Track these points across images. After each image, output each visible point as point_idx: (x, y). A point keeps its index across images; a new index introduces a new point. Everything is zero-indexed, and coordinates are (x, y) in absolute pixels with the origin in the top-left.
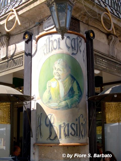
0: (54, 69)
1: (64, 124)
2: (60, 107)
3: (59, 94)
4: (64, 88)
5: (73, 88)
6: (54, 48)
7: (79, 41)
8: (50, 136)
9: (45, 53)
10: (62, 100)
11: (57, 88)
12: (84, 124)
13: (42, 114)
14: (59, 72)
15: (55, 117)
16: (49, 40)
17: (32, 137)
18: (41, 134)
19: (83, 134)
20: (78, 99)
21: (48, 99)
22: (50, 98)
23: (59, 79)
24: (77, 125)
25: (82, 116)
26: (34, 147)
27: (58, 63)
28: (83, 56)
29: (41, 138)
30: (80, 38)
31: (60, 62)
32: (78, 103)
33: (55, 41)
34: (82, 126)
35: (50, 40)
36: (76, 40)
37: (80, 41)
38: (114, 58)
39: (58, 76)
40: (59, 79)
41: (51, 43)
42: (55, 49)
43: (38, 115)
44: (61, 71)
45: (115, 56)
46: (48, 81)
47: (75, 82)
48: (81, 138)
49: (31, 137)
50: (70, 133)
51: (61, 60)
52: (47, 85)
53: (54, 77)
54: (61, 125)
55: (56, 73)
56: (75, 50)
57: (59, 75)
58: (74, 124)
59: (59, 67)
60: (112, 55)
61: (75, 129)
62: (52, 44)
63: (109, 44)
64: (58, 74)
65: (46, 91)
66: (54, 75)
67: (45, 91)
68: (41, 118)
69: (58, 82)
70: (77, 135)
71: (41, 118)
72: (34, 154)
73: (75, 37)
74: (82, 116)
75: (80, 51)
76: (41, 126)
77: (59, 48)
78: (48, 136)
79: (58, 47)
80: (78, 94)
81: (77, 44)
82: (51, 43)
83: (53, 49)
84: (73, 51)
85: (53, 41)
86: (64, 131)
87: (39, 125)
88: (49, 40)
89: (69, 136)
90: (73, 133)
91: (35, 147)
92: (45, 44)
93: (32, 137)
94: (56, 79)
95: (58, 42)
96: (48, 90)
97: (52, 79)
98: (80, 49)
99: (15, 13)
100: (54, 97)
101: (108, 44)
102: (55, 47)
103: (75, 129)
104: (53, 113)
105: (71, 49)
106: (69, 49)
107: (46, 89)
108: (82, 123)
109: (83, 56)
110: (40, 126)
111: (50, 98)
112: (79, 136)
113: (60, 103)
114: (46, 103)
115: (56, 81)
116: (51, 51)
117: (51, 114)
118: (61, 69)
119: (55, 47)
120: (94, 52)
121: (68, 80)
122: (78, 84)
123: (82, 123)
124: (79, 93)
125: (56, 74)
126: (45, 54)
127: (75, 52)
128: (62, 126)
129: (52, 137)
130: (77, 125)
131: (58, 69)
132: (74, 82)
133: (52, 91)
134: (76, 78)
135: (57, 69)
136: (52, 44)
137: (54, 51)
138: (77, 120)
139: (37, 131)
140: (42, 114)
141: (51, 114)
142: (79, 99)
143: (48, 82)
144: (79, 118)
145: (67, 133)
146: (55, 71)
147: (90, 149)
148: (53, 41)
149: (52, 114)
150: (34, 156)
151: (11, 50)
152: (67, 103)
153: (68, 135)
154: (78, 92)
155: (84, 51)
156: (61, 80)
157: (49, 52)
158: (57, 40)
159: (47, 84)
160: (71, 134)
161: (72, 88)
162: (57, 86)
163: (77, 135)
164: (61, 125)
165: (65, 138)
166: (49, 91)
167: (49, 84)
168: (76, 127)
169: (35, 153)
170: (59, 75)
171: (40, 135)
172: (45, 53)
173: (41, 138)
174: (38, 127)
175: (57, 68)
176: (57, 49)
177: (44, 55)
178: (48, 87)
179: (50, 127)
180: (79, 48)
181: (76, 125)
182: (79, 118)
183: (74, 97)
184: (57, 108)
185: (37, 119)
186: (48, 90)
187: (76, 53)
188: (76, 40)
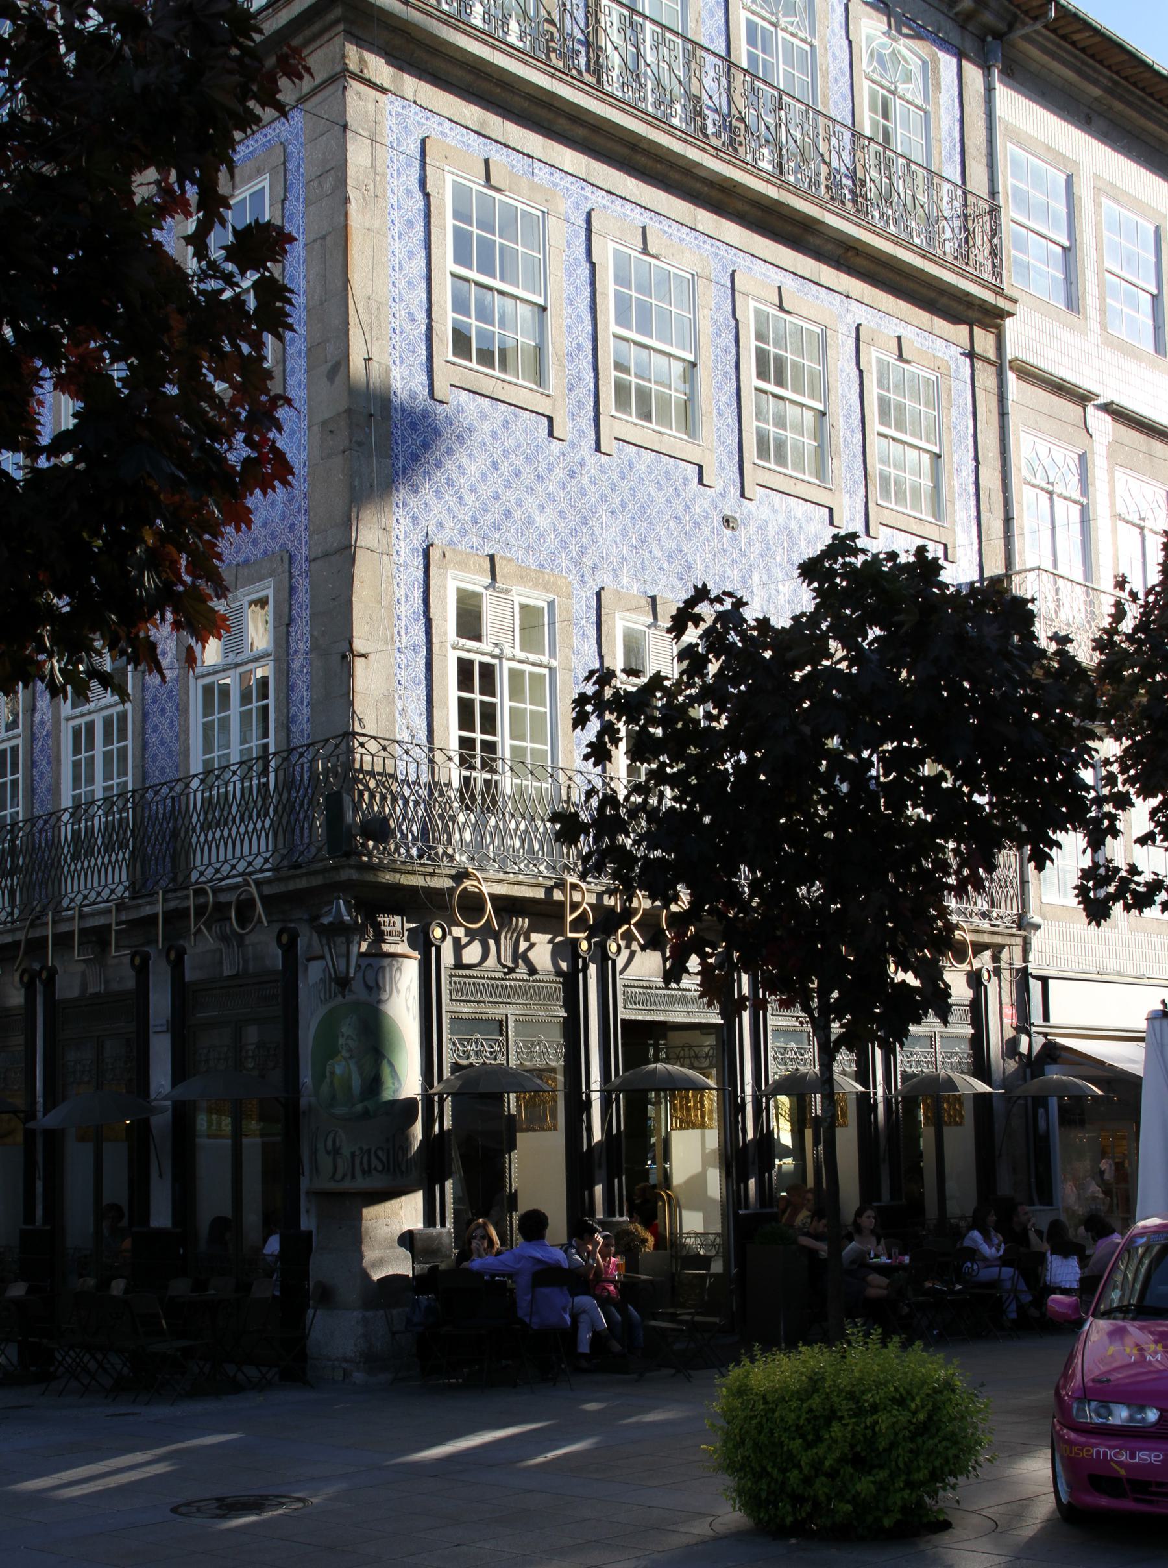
1: (361, 1149)
3: (350, 1088)
14: (350, 1042)
23: (351, 1057)
40: (351, 1057)
52: (328, 1069)
61: (384, 1159)
72: (307, 1212)
86: (361, 1163)
90: (380, 1168)
94: (345, 1058)
96: (328, 1080)
99: (253, 889)
103: (384, 1159)
115: (344, 1063)
129: (339, 1176)
131: (348, 1037)
145: (366, 1167)
146: (341, 1041)
153: (370, 1171)
160: (375, 1168)
166: (332, 1082)
170: (350, 1050)
178: (328, 1074)
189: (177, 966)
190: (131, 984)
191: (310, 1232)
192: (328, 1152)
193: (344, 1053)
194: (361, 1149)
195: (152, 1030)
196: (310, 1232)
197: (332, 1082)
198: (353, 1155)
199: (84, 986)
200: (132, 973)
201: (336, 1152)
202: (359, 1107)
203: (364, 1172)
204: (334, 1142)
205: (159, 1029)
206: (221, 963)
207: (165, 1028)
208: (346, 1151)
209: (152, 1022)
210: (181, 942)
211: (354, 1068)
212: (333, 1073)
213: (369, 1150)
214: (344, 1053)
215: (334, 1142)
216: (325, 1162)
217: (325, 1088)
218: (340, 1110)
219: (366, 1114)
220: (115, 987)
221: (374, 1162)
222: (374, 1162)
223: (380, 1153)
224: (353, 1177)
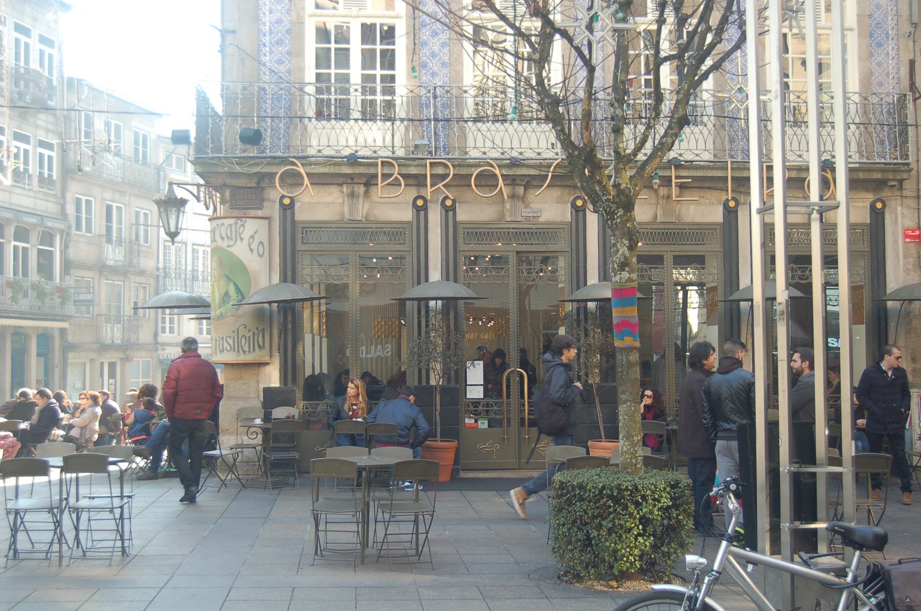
34: (243, 340)
36: (234, 226)
47: (232, 284)
61: (231, 343)
73: (232, 221)
90: (229, 348)
112: (238, 351)
127: (231, 243)
188: (234, 226)
221: (226, 345)
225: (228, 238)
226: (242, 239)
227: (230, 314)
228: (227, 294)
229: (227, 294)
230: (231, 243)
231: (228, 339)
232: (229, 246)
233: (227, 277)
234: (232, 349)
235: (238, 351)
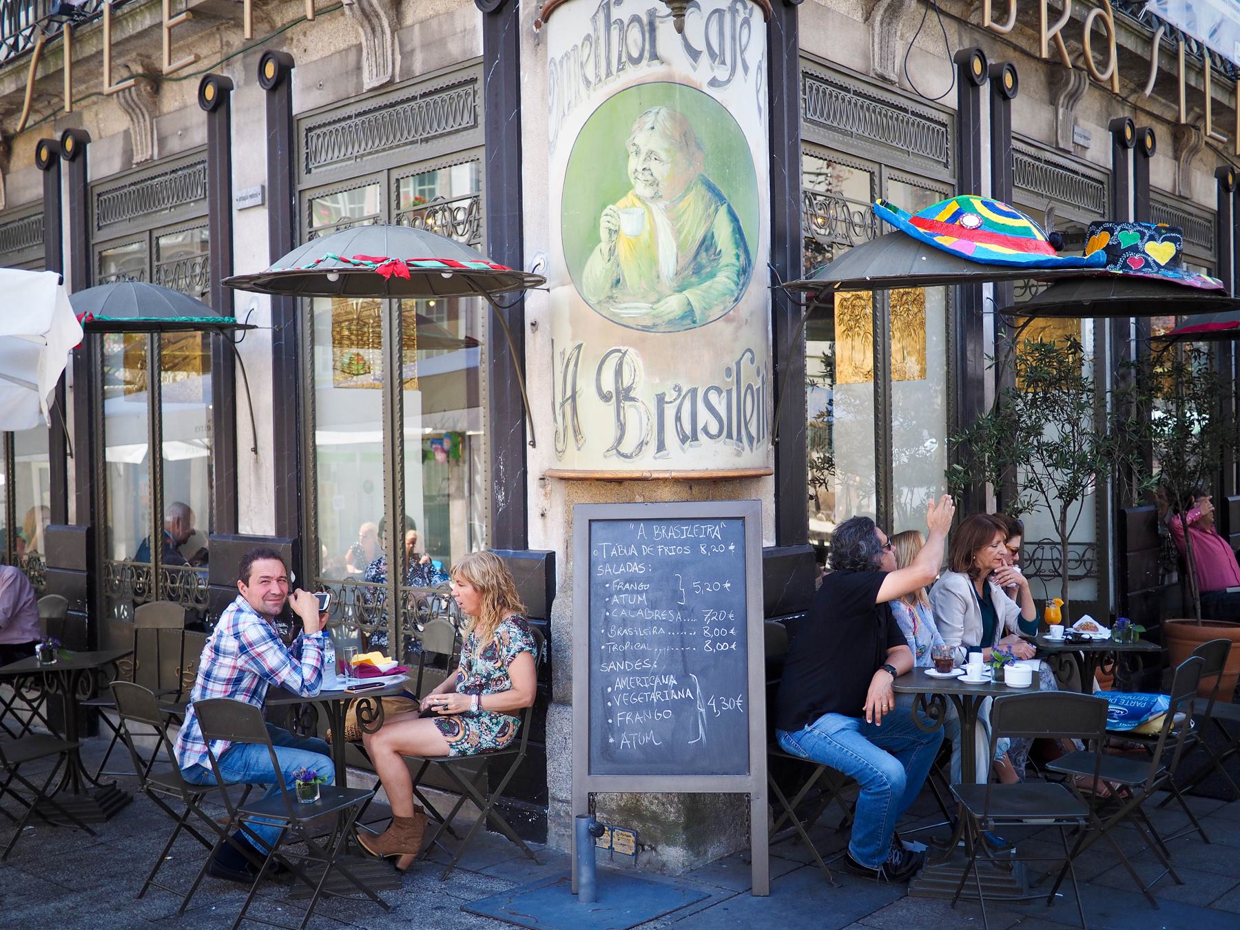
0: (632, 156)
1: (678, 389)
2: (658, 321)
3: (654, 262)
4: (677, 238)
5: (713, 237)
6: (630, 57)
7: (739, 20)
8: (619, 441)
9: (591, 78)
10: (668, 292)
11: (645, 236)
12: (758, 390)
13: (579, 347)
14: (653, 165)
15: (640, 363)
16: (608, 17)
17: (534, 445)
18: (577, 431)
19: (754, 432)
20: (733, 286)
21: (608, 286)
22: (618, 281)
23: (656, 197)
24: (729, 392)
25: (748, 355)
26: (544, 486)
27: (649, 125)
28: (758, 92)
29: (579, 449)
30: (745, 7)
31: (656, 119)
32: (736, 300)
33: (636, 24)
35: (613, 20)
36: (728, 17)
37: (746, 21)
38: (892, 83)
39: (651, 185)
41: (615, 33)
42: (636, 61)
43: (563, 353)
44: (661, 161)
45: (894, 77)
46: (604, 206)
47: (723, 210)
48: (743, 449)
49: (529, 448)
50: (700, 426)
51: (663, 111)
53: (630, 187)
54: (664, 394)
55: (640, 169)
56: (723, 63)
57: (654, 183)
58: (719, 391)
59: (652, 146)
60: (879, 71)
62: (623, 39)
63: (868, 17)
64: (649, 178)
65: (597, 249)
66: (632, 181)
67: (592, 250)
68: (576, 365)
69: (650, 212)
70: (730, 436)
71: (576, 365)
74: (748, 355)
75: (746, 68)
76: (578, 400)
77: (654, 56)
78: (611, 441)
79: (647, 54)
80: (734, 261)
81: (733, 38)
82: (615, 33)
83: (624, 59)
84: (712, 69)
85: (626, 22)
86: (678, 419)
87: (569, 393)
88: (608, 17)
89: (697, 439)
90: (714, 428)
91: (549, 488)
92: (589, 36)
93: (534, 445)
95: (647, 28)
96: (604, 246)
97: (624, 199)
98: (744, 61)
100: (631, 276)
101: (866, 20)
102: (635, 55)
104: (631, 346)
105: (705, 58)
106: (695, 61)
107: (600, 241)
108: (750, 387)
109: (758, 92)
110: (573, 397)
111: (618, 281)
112: (739, 439)
113: (658, 301)
114: (599, 302)
115: (640, 209)
116: (619, 70)
117: (619, 351)
118: (663, 155)
119: (635, 55)
120: (803, 66)
121: (694, 205)
122: (734, 219)
123: (750, 387)
124: (738, 257)
125: (640, 176)
126: (588, 83)
127: (722, 74)
128: (667, 399)
129: (628, 446)
130: (729, 392)
132: (717, 210)
133: (622, 250)
134: (724, 193)
135: (643, 156)
136: (623, 39)
137: (630, 68)
138: (729, 371)
139: (560, 419)
140: (579, 347)
141: (619, 351)
142: (737, 284)
143: (605, 212)
144: (738, 364)
145: (688, 429)
146: (634, 163)
147: (777, 495)
148: (626, 22)
149: (623, 349)
150: (545, 526)
151: (413, 51)
152: (689, 304)
153: (695, 437)
154: (735, 251)
155: (759, 68)
156: (662, 204)
157: (609, 74)
158: (645, 19)
159: (603, 219)
160: (705, 430)
161: (709, 235)
162: (648, 227)
163: (730, 436)
164: (664, 394)
165: (683, 449)
166: (612, 251)
167: (609, 218)
168: (724, 402)
169: (548, 514)
170: (654, 183)
171: (576, 436)
172: (590, 72)
173: (579, 449)
174: (562, 405)
175: (644, 150)
176: (644, 62)
177: (582, 86)
178: (604, 234)
179: (618, 402)
180: (742, 52)
181: (724, 394)
182: (738, 364)
183: (719, 274)
184: (649, 323)
185: (559, 368)
186: (604, 246)
187: (729, 81)
188: (728, 17)
189: (279, 86)
190: (199, 135)
191: (551, 556)
192: (606, 398)
193: (641, 189)
194: (678, 389)
195: (236, 205)
196: (551, 556)
197: (612, 251)
198: (661, 400)
199: (128, 154)
200: (200, 116)
201: (624, 395)
202: (673, 305)
203: (684, 439)
204: (619, 373)
205: (247, 203)
206: (359, 68)
207: (258, 200)
208: (644, 391)
209: (236, 194)
210: (285, 49)
211: (662, 222)
212: (613, 232)
213: (694, 392)
214: (641, 189)
215: (619, 373)
216: (596, 416)
217: (597, 267)
218: (634, 309)
219: (689, 319)
220: (175, 145)
221: (704, 416)
222: (704, 416)
223: (713, 397)
224: (661, 446)
225: (712, 55)
226: (746, 68)
227: (717, 312)
228: (707, 243)
229: (707, 243)
230: (722, 74)
231: (713, 397)
232: (714, 83)
233: (711, 188)
234: (726, 431)
235: (739, 439)
